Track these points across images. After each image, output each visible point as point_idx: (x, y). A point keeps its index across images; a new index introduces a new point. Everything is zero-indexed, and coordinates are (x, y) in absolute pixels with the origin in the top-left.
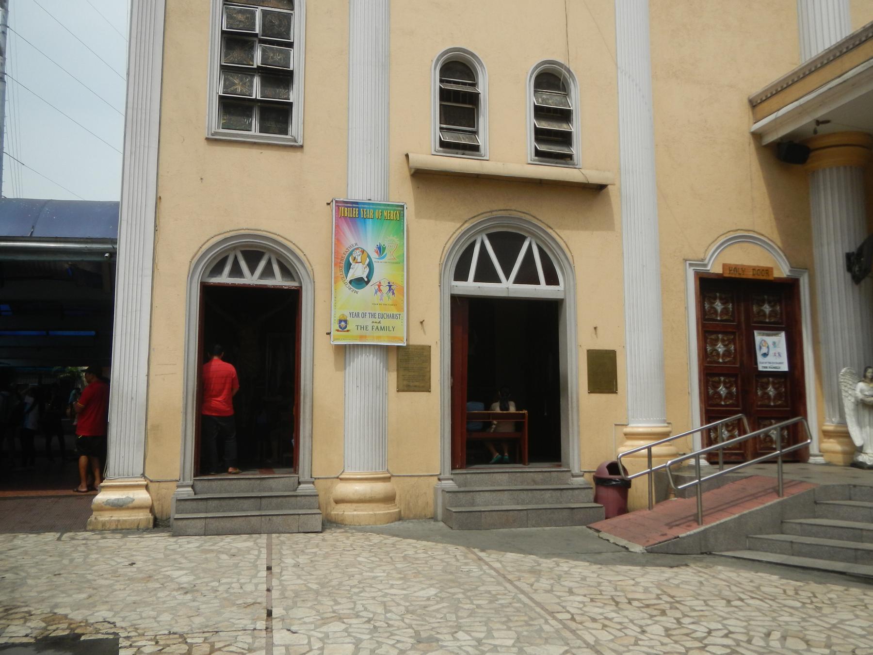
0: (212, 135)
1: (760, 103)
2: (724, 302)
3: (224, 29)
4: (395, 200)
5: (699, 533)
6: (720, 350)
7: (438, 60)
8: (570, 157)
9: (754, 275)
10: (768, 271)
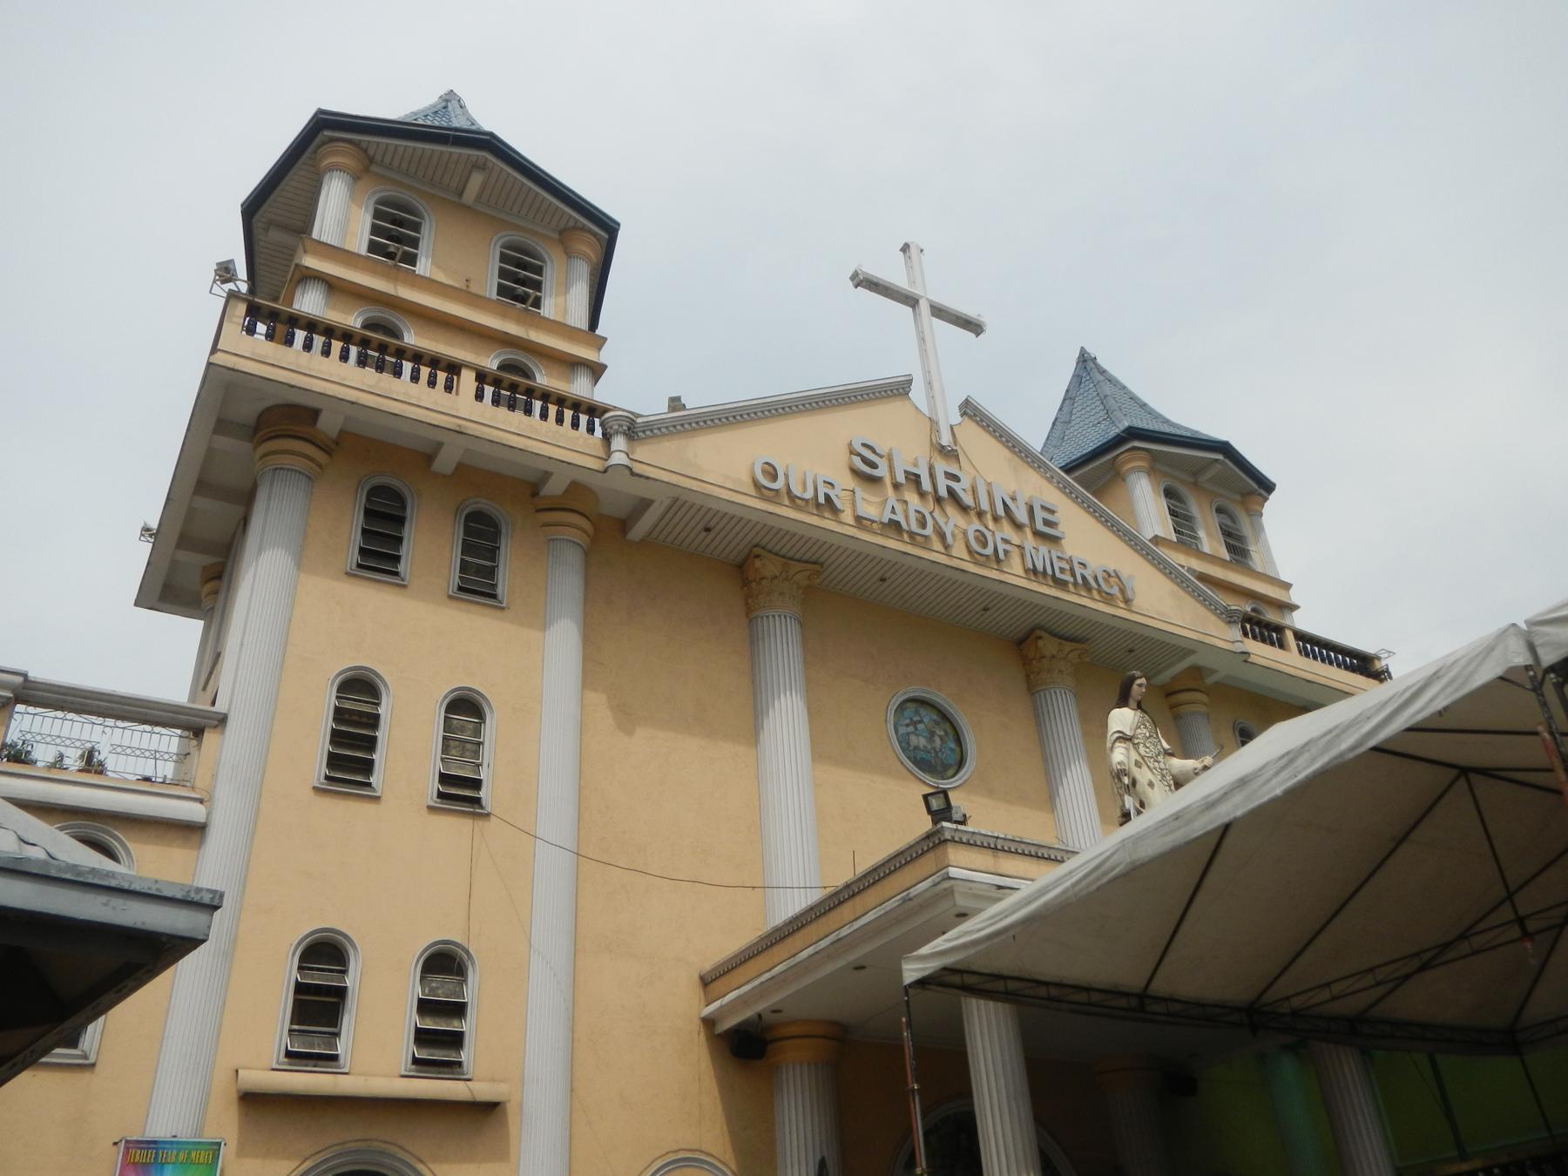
4: (209, 1136)
7: (299, 943)
8: (459, 1064)
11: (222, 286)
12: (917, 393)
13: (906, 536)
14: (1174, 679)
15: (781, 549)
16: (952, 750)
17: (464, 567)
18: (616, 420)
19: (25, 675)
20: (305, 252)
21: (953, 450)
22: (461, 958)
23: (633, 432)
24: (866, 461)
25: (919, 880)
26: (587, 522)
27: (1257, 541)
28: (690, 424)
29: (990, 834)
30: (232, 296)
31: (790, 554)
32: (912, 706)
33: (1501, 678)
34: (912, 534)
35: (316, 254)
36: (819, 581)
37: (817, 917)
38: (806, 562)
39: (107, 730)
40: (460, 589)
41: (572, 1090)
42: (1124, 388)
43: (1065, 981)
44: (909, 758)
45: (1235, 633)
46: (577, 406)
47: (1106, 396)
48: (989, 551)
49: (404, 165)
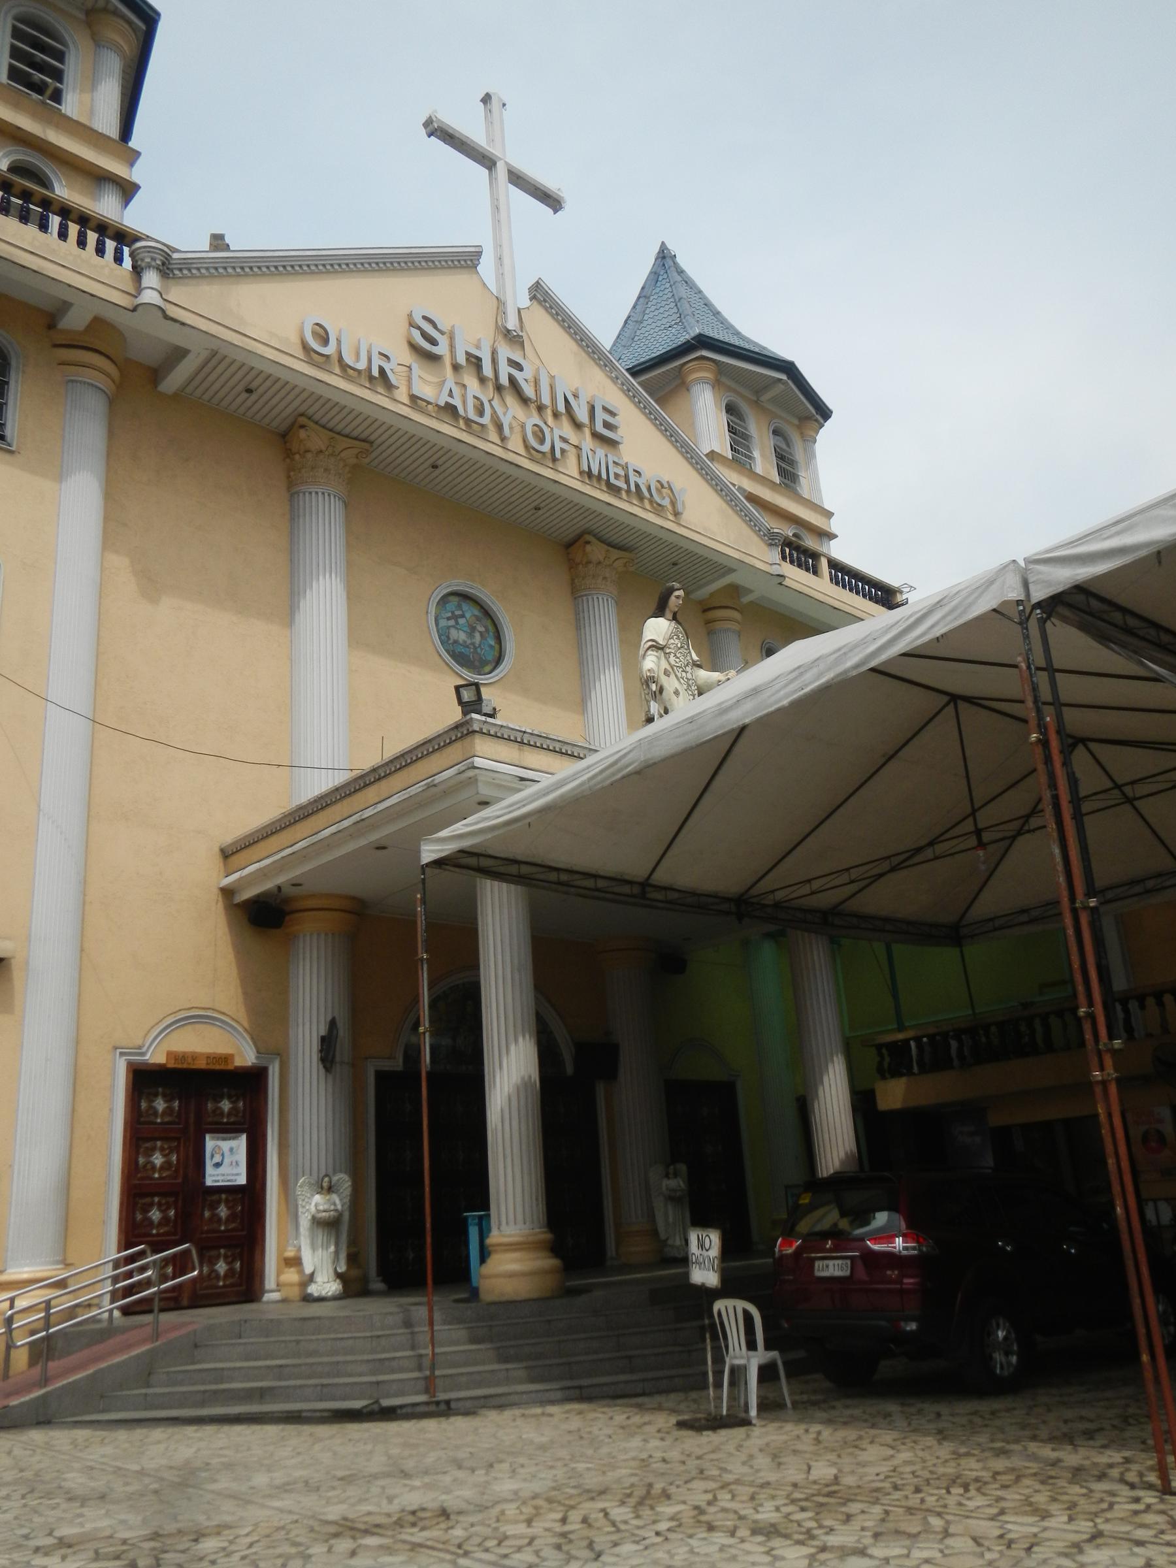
2: (168, 1098)
5: (38, 1398)
6: (156, 1161)
9: (207, 1064)
10: (227, 1058)
12: (486, 266)
13: (462, 424)
14: (712, 595)
15: (329, 421)
16: (491, 647)
23: (168, 269)
24: (424, 335)
25: (445, 768)
26: (113, 366)
27: (807, 469)
28: (234, 268)
29: (517, 728)
31: (339, 428)
32: (455, 600)
33: (994, 610)
34: (468, 421)
36: (367, 460)
37: (342, 798)
38: (356, 439)
41: (82, 950)
42: (700, 292)
43: (575, 868)
44: (447, 651)
45: (774, 555)
46: (103, 228)
47: (680, 299)
48: (546, 448)
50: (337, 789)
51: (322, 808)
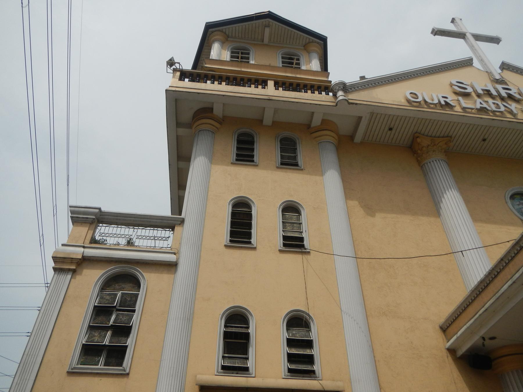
0: (72, 369)
1: (447, 328)
3: (96, 304)
8: (313, 372)
11: (171, 68)
13: (491, 114)
15: (428, 132)
17: (282, 157)
18: (337, 85)
19: (100, 209)
20: (205, 64)
21: (502, 80)
22: (306, 319)
23: (346, 89)
28: (371, 84)
30: (175, 70)
31: (434, 135)
34: (494, 112)
35: (209, 64)
37: (507, 264)
38: (443, 137)
39: (136, 230)
40: (282, 164)
49: (240, 35)
50: (502, 259)
51: (496, 276)
